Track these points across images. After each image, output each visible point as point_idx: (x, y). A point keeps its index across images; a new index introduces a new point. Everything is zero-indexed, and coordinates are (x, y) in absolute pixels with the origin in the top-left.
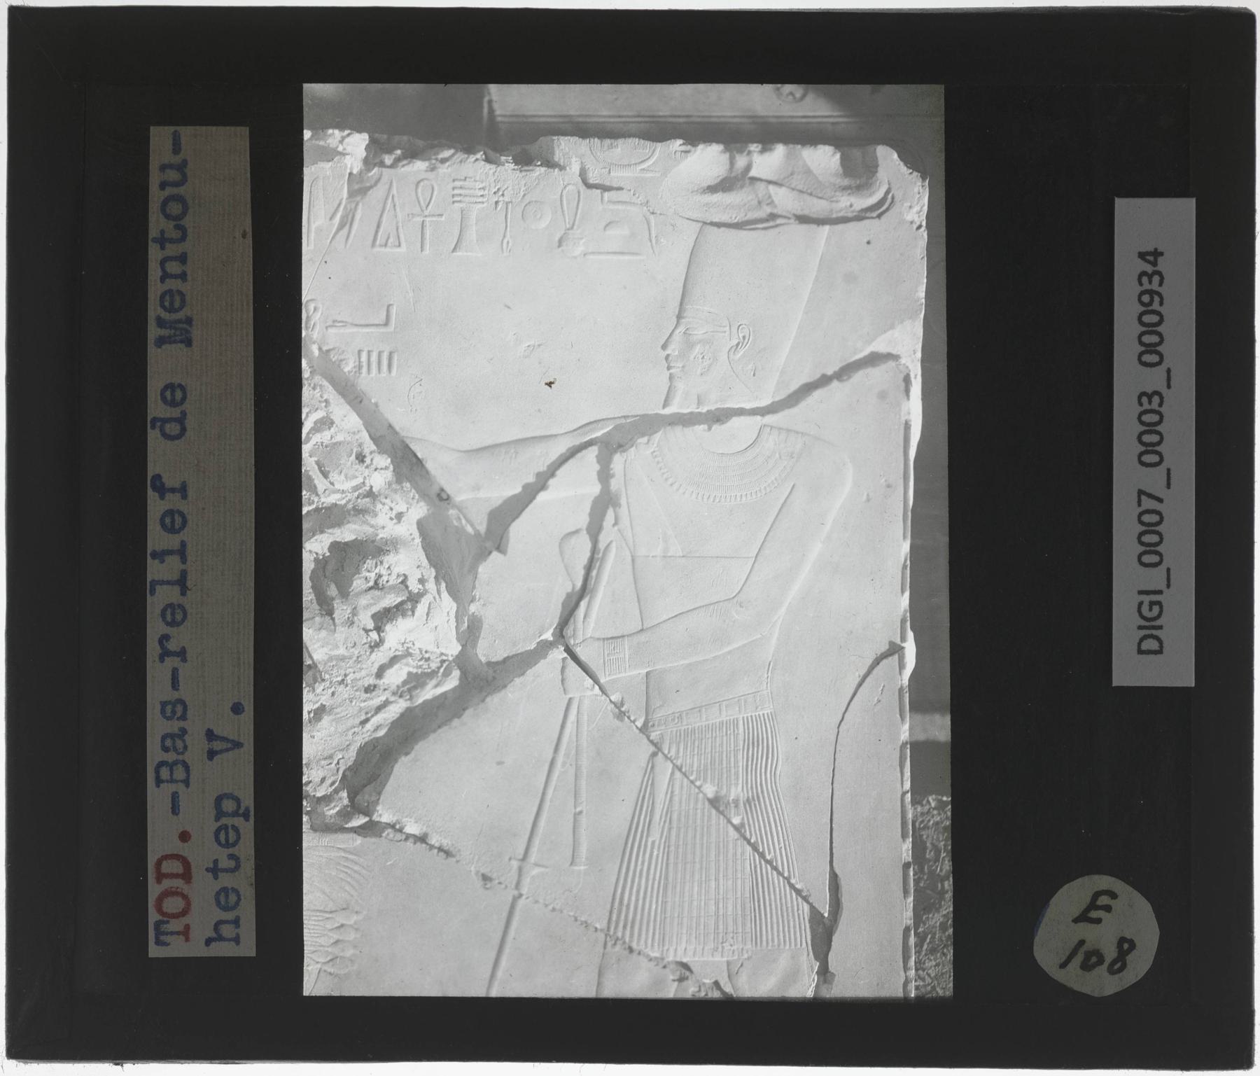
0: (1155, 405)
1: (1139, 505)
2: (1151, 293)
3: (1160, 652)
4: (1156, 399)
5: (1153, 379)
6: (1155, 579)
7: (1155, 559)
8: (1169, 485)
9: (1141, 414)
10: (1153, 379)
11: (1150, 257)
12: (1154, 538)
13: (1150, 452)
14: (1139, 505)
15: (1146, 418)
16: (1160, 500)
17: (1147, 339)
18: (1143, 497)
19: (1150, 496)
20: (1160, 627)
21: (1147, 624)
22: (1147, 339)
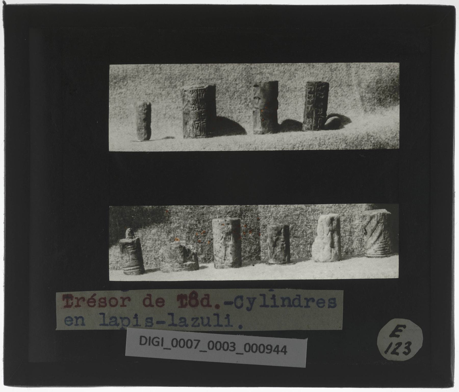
0: (230, 348)
2: (271, 349)
4: (232, 349)
5: (240, 348)
7: (175, 344)
8: (201, 351)
9: (227, 343)
10: (240, 348)
15: (226, 346)
17: (254, 347)
19: (198, 344)
22: (254, 347)
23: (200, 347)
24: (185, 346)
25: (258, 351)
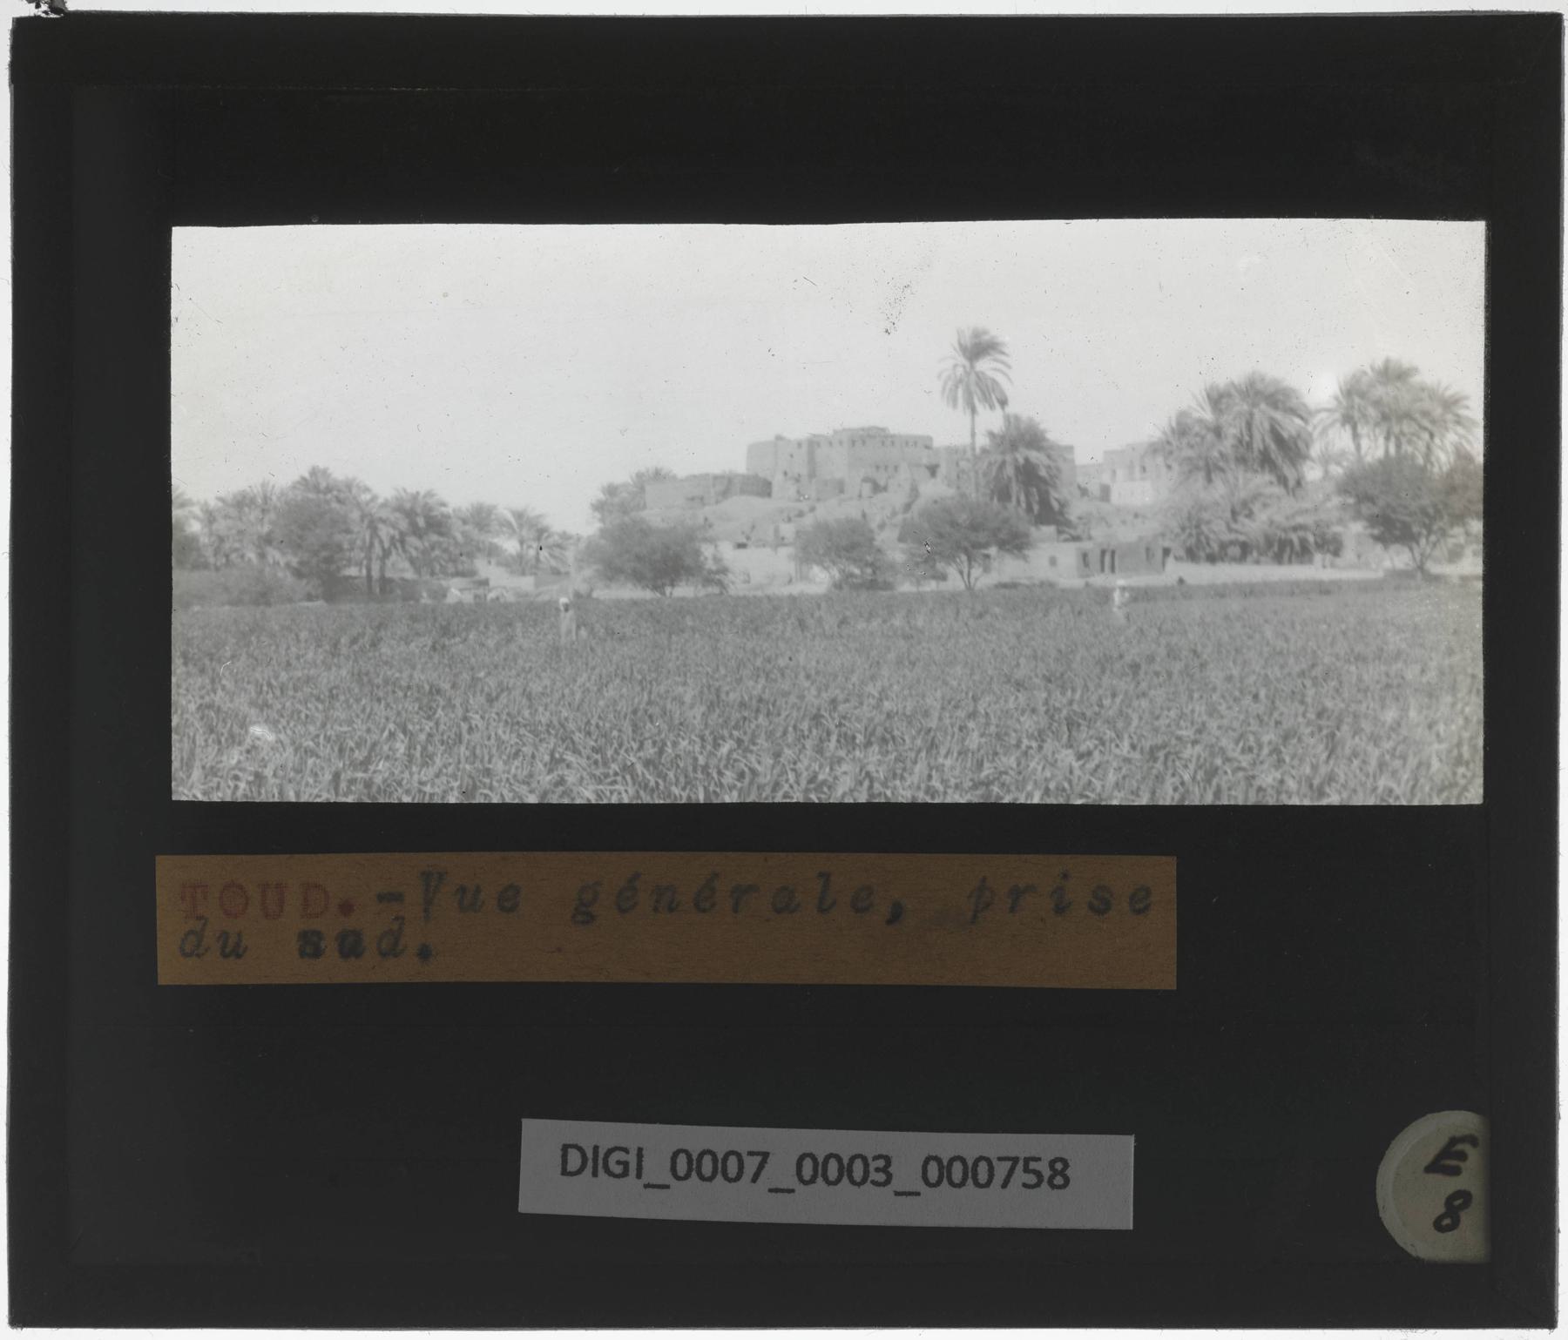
0: (874, 1176)
1: (751, 1154)
3: (565, 1172)
4: (881, 1177)
5: (906, 1174)
6: (657, 1169)
8: (771, 1191)
9: (864, 1159)
10: (906, 1174)
11: (1059, 1174)
13: (814, 1170)
14: (751, 1154)
15: (858, 1168)
16: (754, 1180)
18: (759, 1159)
20: (595, 1174)
25: (970, 1181)
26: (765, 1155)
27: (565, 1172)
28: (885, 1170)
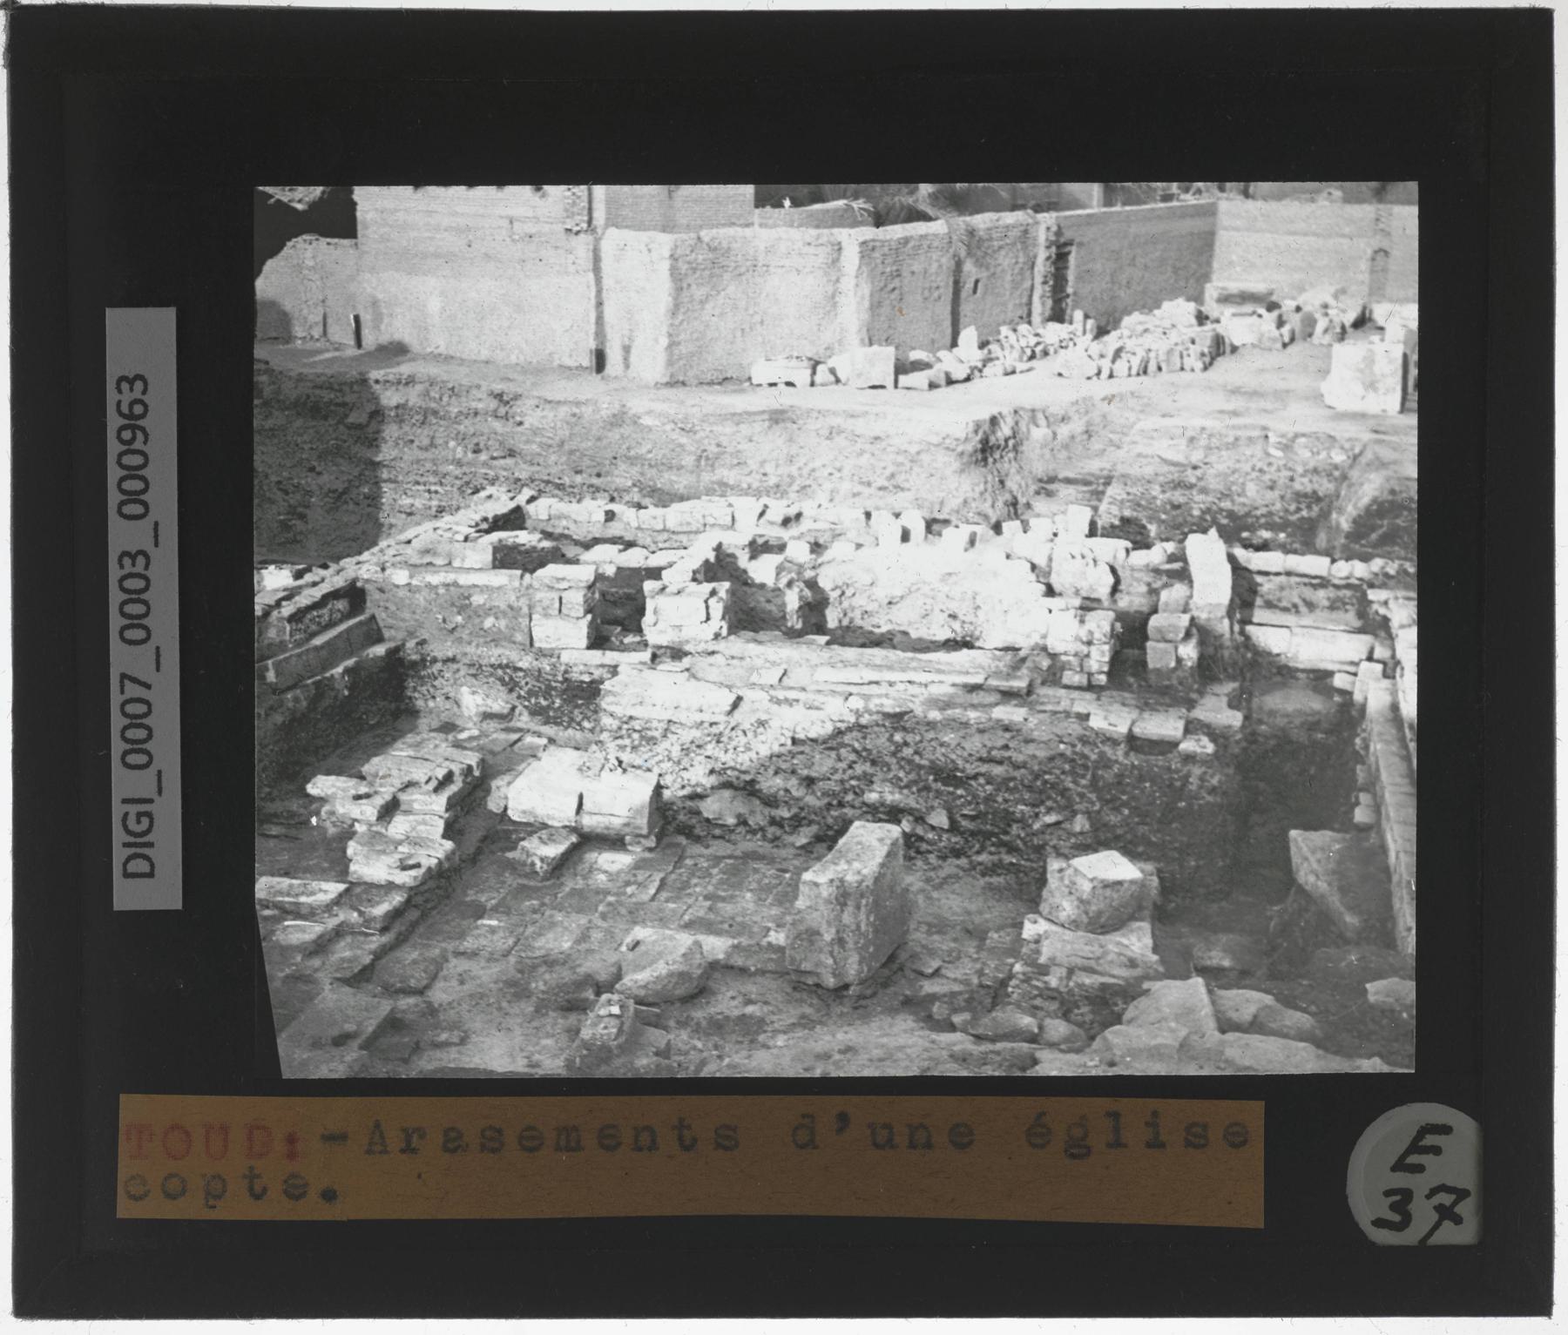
0: (139, 568)
1: (122, 692)
3: (151, 875)
4: (141, 560)
6: (141, 783)
8: (158, 669)
12: (141, 734)
14: (122, 692)
15: (129, 584)
16: (148, 687)
17: (130, 485)
18: (127, 682)
19: (135, 680)
20: (151, 845)
21: (132, 839)
22: (130, 485)
23: (145, 671)
24: (145, 721)
26: (124, 676)
27: (151, 875)
28: (133, 557)
